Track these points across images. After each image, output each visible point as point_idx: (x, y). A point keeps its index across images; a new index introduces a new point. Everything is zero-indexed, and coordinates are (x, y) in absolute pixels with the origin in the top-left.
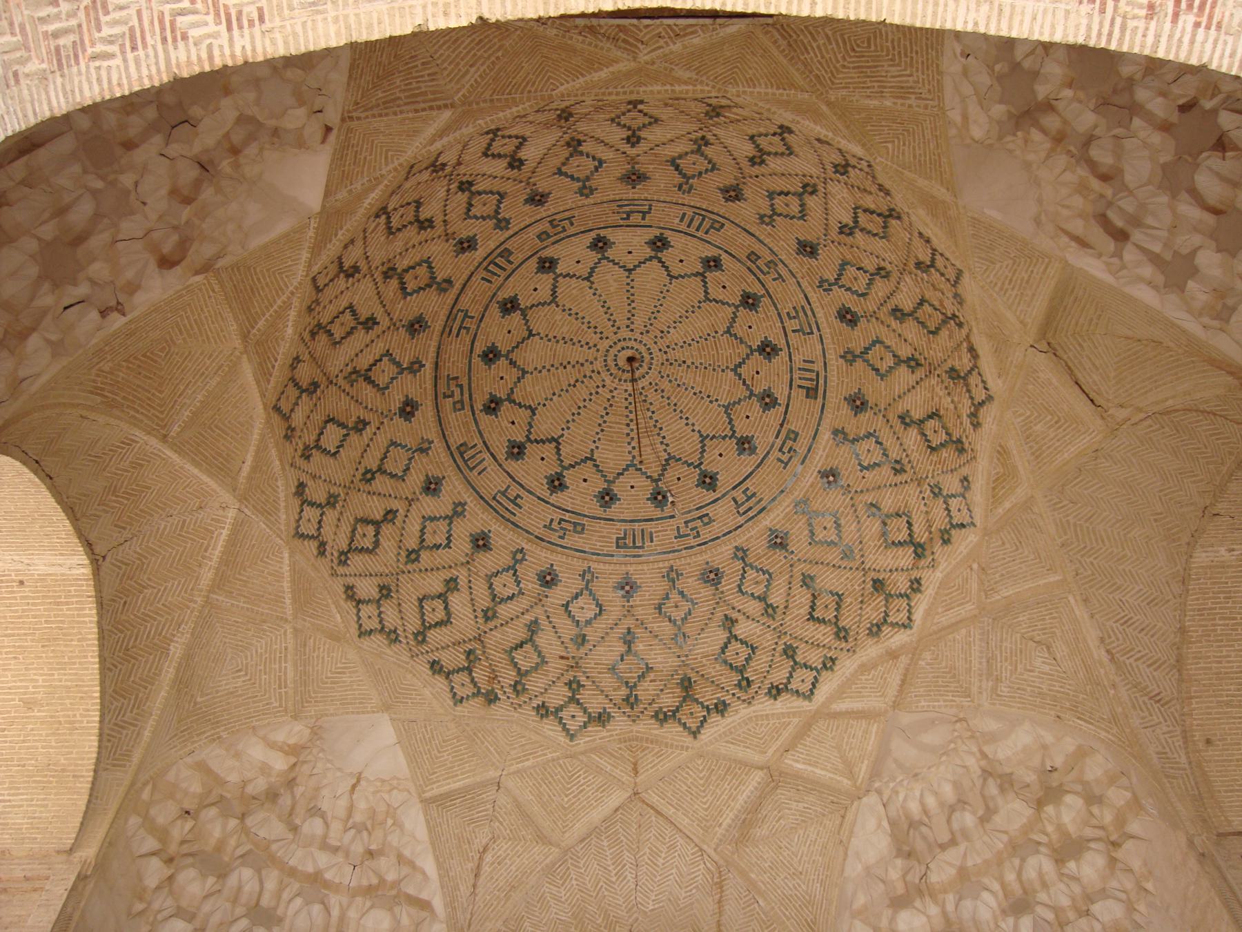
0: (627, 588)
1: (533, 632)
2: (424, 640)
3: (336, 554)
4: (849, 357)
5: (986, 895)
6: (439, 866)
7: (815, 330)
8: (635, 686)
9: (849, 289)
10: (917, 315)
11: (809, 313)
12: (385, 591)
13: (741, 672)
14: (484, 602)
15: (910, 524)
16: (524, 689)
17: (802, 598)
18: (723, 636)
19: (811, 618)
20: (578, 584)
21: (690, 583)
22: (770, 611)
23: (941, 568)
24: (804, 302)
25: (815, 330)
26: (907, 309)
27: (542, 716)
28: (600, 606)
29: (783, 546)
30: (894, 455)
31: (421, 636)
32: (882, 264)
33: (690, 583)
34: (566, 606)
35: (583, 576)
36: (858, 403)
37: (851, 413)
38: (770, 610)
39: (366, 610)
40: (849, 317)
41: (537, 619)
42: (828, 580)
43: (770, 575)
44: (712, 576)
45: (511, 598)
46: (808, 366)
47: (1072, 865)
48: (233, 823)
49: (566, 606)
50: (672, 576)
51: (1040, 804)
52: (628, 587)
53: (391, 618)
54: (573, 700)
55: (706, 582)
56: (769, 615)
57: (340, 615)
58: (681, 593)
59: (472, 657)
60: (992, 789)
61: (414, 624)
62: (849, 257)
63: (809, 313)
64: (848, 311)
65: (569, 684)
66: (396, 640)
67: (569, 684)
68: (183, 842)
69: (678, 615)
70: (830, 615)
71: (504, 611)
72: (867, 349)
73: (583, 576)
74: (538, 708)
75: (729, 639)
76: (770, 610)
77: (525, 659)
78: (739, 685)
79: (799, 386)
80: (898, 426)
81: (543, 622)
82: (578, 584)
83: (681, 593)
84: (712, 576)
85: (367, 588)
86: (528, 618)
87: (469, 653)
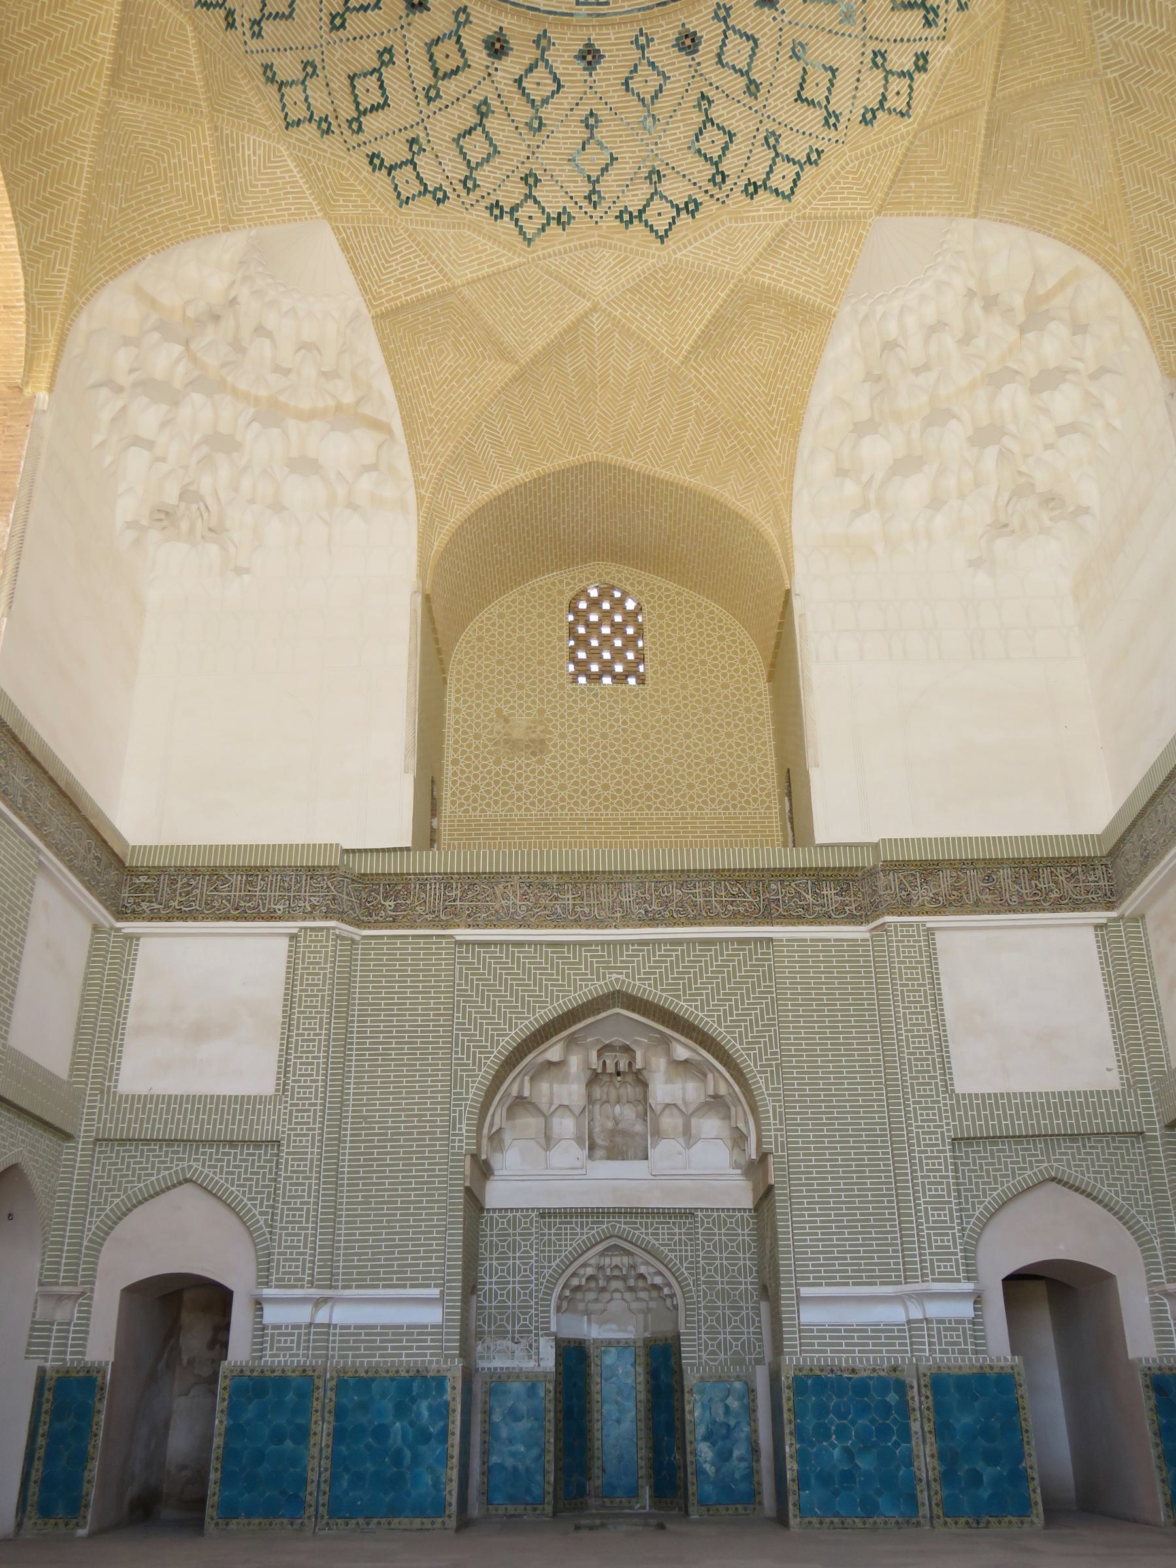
0: (589, 58)
1: (483, 115)
2: (360, 129)
3: (248, 25)
6: (396, 387)
8: (598, 181)
12: (310, 68)
13: (716, 164)
14: (424, 76)
16: (476, 186)
17: (790, 71)
18: (698, 118)
19: (799, 98)
20: (532, 54)
21: (663, 51)
22: (753, 87)
23: (953, 41)
27: (496, 218)
28: (556, 79)
31: (355, 125)
33: (663, 51)
34: (519, 81)
35: (537, 42)
38: (753, 88)
39: (294, 94)
41: (485, 102)
42: (823, 50)
43: (755, 41)
44: (688, 43)
45: (455, 72)
47: (1045, 395)
48: (177, 349)
49: (519, 81)
50: (642, 44)
51: (1023, 330)
52: (590, 56)
53: (321, 105)
54: (529, 196)
55: (680, 50)
56: (751, 94)
57: (260, 102)
58: (652, 65)
59: (415, 148)
60: (977, 308)
61: (347, 111)
65: (525, 179)
66: (328, 131)
67: (525, 179)
68: (131, 371)
69: (647, 92)
70: (819, 95)
71: (449, 88)
73: (537, 42)
74: (490, 208)
75: (704, 122)
76: (753, 88)
77: (476, 147)
78: (712, 180)
81: (494, 103)
82: (532, 54)
83: (652, 65)
84: (688, 42)
85: (288, 67)
86: (477, 96)
87: (413, 141)
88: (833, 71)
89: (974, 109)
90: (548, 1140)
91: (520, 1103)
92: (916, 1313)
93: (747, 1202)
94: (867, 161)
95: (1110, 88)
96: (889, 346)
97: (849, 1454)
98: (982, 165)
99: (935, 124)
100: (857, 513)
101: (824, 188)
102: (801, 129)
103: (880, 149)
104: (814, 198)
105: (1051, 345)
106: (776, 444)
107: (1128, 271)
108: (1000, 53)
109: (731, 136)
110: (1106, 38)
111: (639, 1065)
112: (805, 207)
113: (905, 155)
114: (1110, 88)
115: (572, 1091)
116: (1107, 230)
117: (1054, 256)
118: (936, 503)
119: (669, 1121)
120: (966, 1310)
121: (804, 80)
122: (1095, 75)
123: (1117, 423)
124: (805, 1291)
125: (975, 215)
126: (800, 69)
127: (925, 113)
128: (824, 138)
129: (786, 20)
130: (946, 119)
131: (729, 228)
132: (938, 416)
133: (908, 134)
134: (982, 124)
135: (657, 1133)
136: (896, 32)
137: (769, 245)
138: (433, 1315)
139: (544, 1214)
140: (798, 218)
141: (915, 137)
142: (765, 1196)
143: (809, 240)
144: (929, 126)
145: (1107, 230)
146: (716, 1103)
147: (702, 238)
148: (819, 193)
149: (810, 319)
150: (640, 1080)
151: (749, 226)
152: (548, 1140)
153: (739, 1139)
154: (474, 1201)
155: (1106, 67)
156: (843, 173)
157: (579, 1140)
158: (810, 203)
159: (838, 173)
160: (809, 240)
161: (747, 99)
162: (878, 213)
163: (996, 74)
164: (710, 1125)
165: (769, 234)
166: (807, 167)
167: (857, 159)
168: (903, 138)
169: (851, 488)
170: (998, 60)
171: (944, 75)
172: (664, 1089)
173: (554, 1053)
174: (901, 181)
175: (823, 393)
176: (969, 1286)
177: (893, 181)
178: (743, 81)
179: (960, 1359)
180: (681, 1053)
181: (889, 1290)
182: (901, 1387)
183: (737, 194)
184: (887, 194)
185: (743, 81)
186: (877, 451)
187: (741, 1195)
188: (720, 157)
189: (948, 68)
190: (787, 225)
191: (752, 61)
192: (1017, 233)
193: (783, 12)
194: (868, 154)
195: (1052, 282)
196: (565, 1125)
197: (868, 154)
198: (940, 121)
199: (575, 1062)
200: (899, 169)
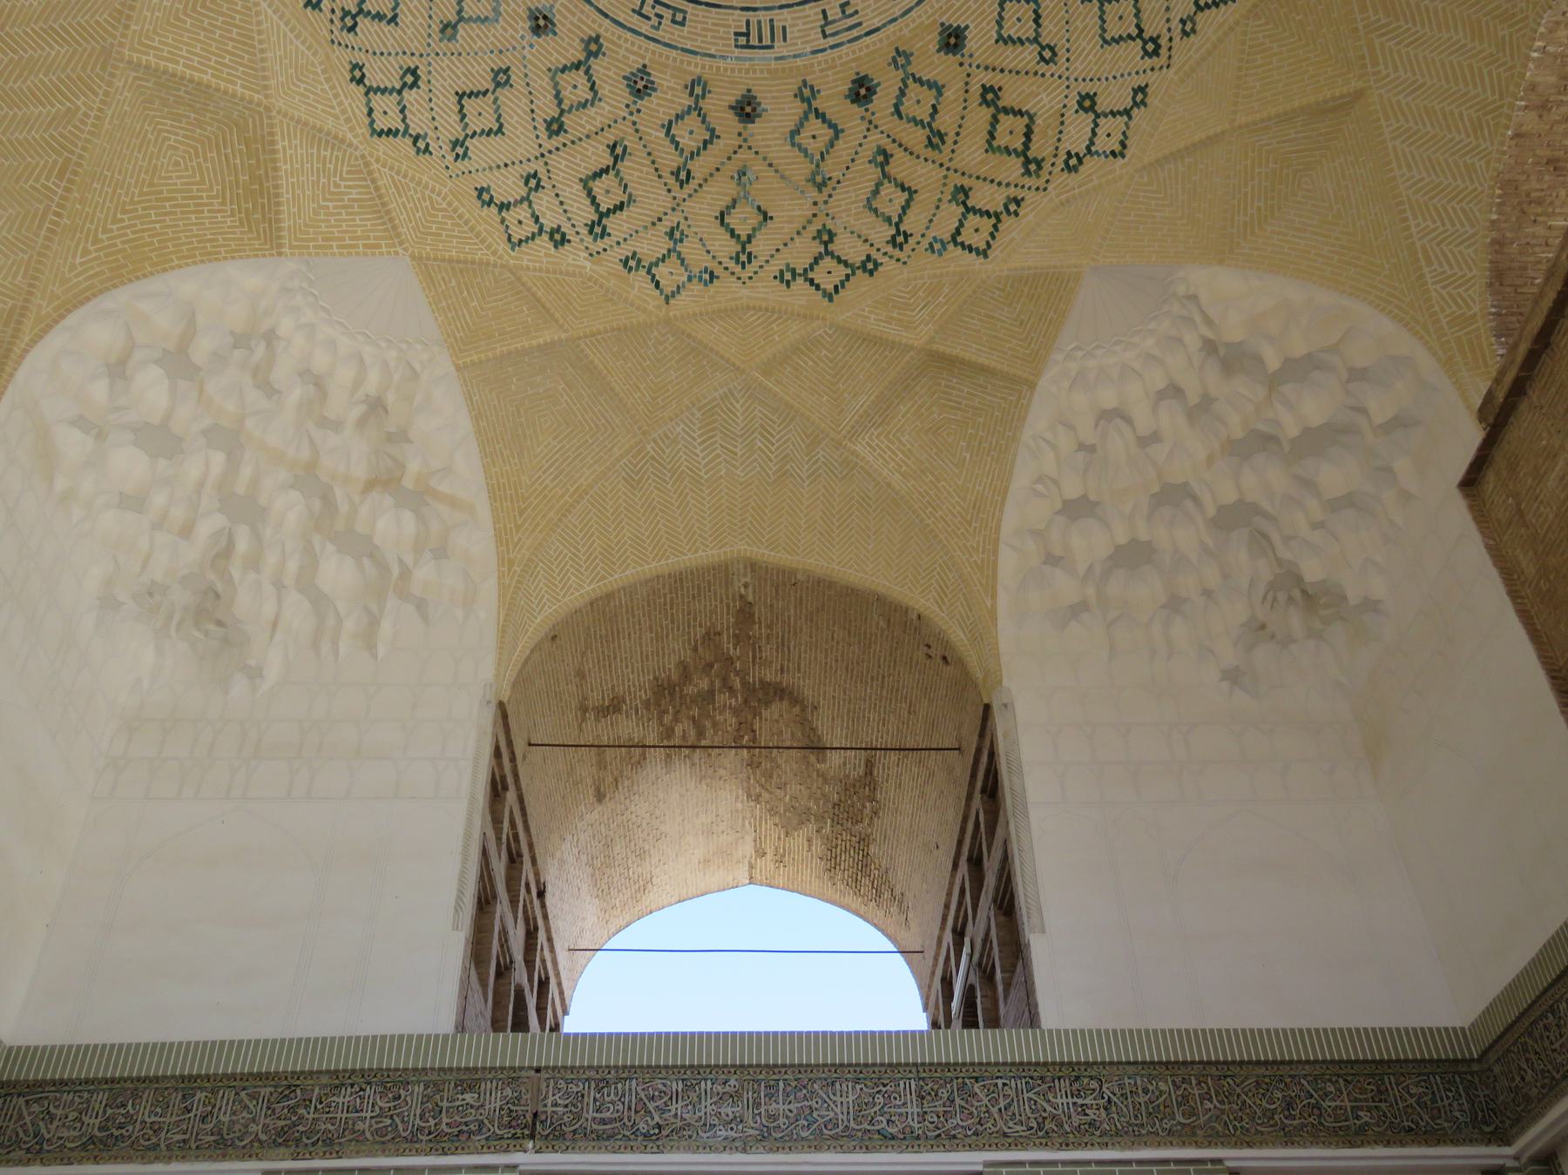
4: (807, 94)
5: (218, 459)
7: (831, 41)
9: (902, 93)
10: (886, 184)
11: (855, 33)
15: (620, 207)
19: (461, 96)
24: (866, 27)
25: (831, 41)
26: (891, 169)
29: (537, 30)
30: (699, 167)
32: (949, 140)
36: (748, 109)
37: (732, 99)
40: (863, 91)
46: (778, 33)
56: (442, 31)
62: (949, 94)
63: (855, 33)
64: (871, 91)
72: (820, 115)
79: (748, 23)
80: (731, 168)
88: (500, 130)
89: (557, 321)
94: (451, 218)
95: (639, 452)
96: (270, 337)
98: (510, 353)
99: (523, 284)
100: (79, 422)
101: (405, 176)
102: (431, 111)
103: (472, 229)
104: (391, 169)
105: (390, 526)
106: (86, 252)
107: (511, 563)
108: (619, 329)
109: (393, 20)
110: (679, 429)
112: (377, 161)
113: (481, 263)
114: (639, 452)
116: (521, 515)
117: (466, 476)
118: (133, 502)
121: (477, 95)
122: (644, 433)
123: (381, 651)
125: (458, 369)
126: (487, 86)
127: (528, 268)
128: (440, 148)
129: (525, 52)
130: (533, 295)
131: (313, 65)
132: (229, 439)
133: (500, 257)
134: (546, 336)
136: (566, 194)
137: (320, 130)
140: (363, 157)
141: (503, 266)
143: (342, 179)
144: (519, 279)
145: (521, 515)
147: (292, 31)
148: (398, 173)
149: (258, 219)
151: (323, 90)
155: (655, 441)
156: (427, 192)
158: (384, 166)
159: (426, 187)
160: (342, 179)
161: (436, 28)
162: (413, 257)
163: (599, 333)
165: (330, 124)
166: (409, 141)
167: (449, 204)
168: (494, 253)
169: (100, 391)
170: (613, 330)
171: (567, 274)
174: (453, 269)
175: (187, 284)
177: (450, 261)
178: (453, 18)
183: (346, 57)
184: (435, 259)
185: (453, 18)
186: (152, 390)
188: (369, 13)
189: (574, 275)
190: (350, 145)
191: (475, 21)
192: (465, 424)
193: (531, 46)
194: (460, 216)
195: (444, 488)
197: (460, 216)
198: (529, 290)
200: (465, 262)
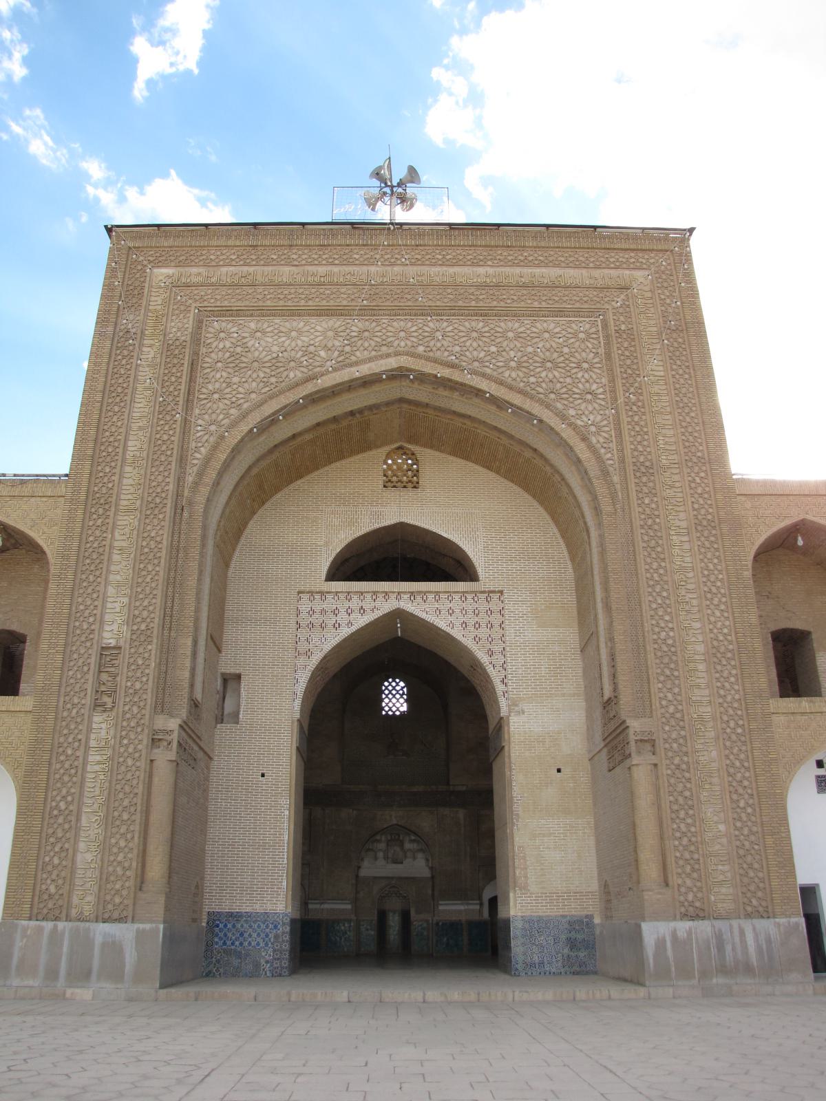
90: (376, 858)
91: (369, 850)
92: (466, 907)
93: (429, 875)
97: (448, 939)
111: (401, 838)
115: (382, 846)
119: (409, 854)
120: (478, 907)
124: (440, 902)
135: (406, 857)
138: (349, 907)
139: (375, 878)
142: (433, 877)
146: (421, 850)
150: (402, 845)
152: (376, 858)
153: (427, 860)
154: (357, 876)
157: (384, 858)
164: (420, 855)
172: (407, 846)
173: (378, 837)
176: (478, 902)
179: (476, 918)
180: (413, 838)
181: (459, 902)
182: (462, 924)
187: (426, 873)
196: (381, 854)
199: (383, 838)
